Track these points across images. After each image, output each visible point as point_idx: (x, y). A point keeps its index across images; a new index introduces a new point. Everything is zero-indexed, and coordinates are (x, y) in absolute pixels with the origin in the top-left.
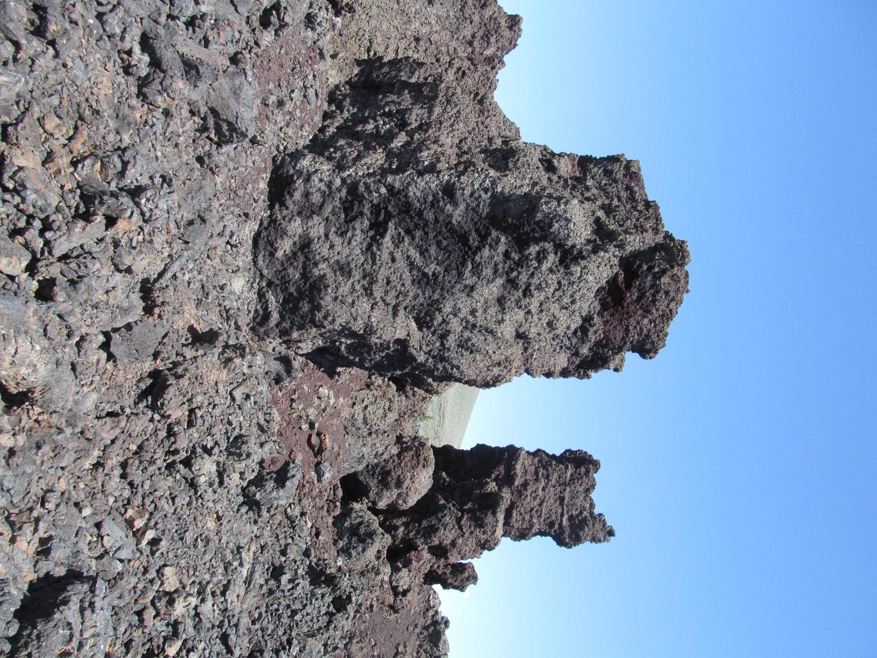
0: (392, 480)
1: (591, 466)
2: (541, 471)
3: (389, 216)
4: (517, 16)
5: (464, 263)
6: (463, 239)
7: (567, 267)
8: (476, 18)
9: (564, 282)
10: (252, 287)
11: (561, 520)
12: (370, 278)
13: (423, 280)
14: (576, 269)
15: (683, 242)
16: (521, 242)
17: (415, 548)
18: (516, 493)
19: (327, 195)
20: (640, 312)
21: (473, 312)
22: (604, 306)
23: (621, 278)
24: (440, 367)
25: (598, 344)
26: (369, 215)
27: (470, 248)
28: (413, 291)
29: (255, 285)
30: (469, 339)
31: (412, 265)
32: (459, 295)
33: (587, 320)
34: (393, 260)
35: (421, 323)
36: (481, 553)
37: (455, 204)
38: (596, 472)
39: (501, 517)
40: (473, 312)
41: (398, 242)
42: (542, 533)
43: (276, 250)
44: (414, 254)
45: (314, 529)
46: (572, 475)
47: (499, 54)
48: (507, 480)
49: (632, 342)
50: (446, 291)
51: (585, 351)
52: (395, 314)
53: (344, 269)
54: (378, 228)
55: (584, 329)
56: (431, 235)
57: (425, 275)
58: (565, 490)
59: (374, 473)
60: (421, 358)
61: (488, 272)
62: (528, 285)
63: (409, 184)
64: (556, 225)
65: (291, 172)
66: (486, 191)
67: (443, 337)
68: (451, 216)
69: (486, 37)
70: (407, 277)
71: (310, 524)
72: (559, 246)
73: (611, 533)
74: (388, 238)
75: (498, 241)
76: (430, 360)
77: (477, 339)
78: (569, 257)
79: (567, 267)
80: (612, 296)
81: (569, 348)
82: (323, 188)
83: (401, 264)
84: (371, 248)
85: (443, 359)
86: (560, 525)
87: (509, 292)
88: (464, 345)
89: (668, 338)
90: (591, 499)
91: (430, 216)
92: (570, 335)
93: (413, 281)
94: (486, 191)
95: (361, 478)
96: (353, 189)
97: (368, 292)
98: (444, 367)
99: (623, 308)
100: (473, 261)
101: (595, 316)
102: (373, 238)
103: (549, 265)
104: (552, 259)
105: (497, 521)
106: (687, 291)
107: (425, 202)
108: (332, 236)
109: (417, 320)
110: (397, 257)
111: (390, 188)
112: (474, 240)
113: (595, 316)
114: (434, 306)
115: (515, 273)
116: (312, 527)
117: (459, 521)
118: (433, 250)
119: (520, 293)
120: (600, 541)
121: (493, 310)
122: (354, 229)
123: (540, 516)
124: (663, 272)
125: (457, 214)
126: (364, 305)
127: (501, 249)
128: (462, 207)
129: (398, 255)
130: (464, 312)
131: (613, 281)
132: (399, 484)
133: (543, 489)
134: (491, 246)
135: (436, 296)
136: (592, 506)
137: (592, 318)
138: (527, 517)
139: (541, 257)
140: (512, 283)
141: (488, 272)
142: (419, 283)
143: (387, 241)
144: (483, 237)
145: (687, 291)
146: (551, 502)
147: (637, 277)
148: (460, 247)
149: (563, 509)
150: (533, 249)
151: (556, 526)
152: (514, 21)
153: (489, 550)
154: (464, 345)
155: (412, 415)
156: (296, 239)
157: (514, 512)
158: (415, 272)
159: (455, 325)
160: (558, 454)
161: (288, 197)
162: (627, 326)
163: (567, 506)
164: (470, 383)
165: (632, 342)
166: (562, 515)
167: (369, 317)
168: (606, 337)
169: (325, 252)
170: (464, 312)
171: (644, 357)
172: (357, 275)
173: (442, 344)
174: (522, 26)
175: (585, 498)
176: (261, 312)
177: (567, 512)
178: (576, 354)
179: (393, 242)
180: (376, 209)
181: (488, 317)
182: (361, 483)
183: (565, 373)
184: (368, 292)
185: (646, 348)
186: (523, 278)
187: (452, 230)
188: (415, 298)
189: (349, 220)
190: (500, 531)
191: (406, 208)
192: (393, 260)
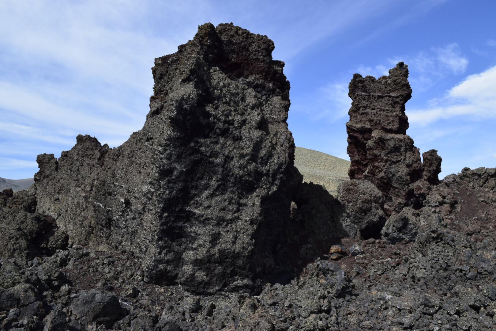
1: (357, 79)
2: (361, 111)
3: (182, 210)
4: (77, 138)
5: (213, 163)
9: (224, 101)
10: (228, 296)
11: (393, 97)
13: (221, 189)
15: (199, 27)
18: (376, 127)
20: (244, 53)
21: (242, 156)
26: (181, 223)
27: (202, 159)
29: (227, 294)
31: (212, 196)
32: (231, 166)
34: (209, 207)
36: (416, 148)
37: (175, 168)
38: (361, 76)
39: (390, 136)
41: (198, 205)
42: (403, 109)
43: (203, 281)
44: (206, 193)
45: (392, 256)
46: (364, 92)
47: (99, 148)
48: (366, 132)
49: (264, 56)
52: (245, 205)
53: (215, 238)
54: (189, 217)
55: (256, 87)
56: (194, 184)
57: (218, 187)
58: (373, 95)
59: (360, 218)
60: (275, 188)
62: (225, 122)
63: (161, 198)
64: (185, 106)
65: (154, 272)
66: (165, 150)
68: (182, 172)
71: (389, 259)
74: (196, 211)
76: (276, 182)
77: (263, 152)
79: (214, 99)
80: (235, 70)
81: (269, 97)
82: (165, 251)
86: (396, 97)
87: (230, 134)
89: (261, 34)
90: (380, 79)
92: (260, 95)
93: (222, 194)
94: (165, 150)
95: (364, 226)
98: (281, 173)
99: (241, 63)
100: (210, 157)
101: (248, 80)
102: (197, 219)
103: (212, 110)
105: (393, 138)
106: (232, 24)
107: (172, 188)
108: (194, 246)
110: (206, 204)
113: (248, 80)
114: (239, 181)
115: (218, 130)
116: (391, 258)
118: (203, 183)
120: (407, 71)
121: (242, 144)
122: (191, 232)
125: (179, 168)
128: (176, 165)
129: (206, 204)
133: (373, 109)
134: (201, 146)
135: (232, 180)
136: (384, 77)
137: (249, 82)
140: (225, 133)
142: (224, 190)
145: (232, 24)
149: (386, 96)
150: (203, 121)
151: (397, 100)
152: (80, 139)
153: (413, 142)
156: (196, 268)
157: (388, 128)
158: (217, 193)
159: (251, 167)
160: (352, 101)
161: (170, 274)
162: (254, 59)
163: (384, 93)
164: (291, 156)
165: (264, 56)
166: (390, 96)
167: (246, 221)
168: (261, 73)
169: (204, 250)
171: (273, 48)
174: (84, 135)
175: (378, 83)
176: (244, 290)
177: (388, 93)
179: (199, 207)
182: (367, 227)
183: (286, 98)
185: (269, 46)
186: (221, 125)
188: (232, 192)
190: (400, 136)
192: (209, 207)
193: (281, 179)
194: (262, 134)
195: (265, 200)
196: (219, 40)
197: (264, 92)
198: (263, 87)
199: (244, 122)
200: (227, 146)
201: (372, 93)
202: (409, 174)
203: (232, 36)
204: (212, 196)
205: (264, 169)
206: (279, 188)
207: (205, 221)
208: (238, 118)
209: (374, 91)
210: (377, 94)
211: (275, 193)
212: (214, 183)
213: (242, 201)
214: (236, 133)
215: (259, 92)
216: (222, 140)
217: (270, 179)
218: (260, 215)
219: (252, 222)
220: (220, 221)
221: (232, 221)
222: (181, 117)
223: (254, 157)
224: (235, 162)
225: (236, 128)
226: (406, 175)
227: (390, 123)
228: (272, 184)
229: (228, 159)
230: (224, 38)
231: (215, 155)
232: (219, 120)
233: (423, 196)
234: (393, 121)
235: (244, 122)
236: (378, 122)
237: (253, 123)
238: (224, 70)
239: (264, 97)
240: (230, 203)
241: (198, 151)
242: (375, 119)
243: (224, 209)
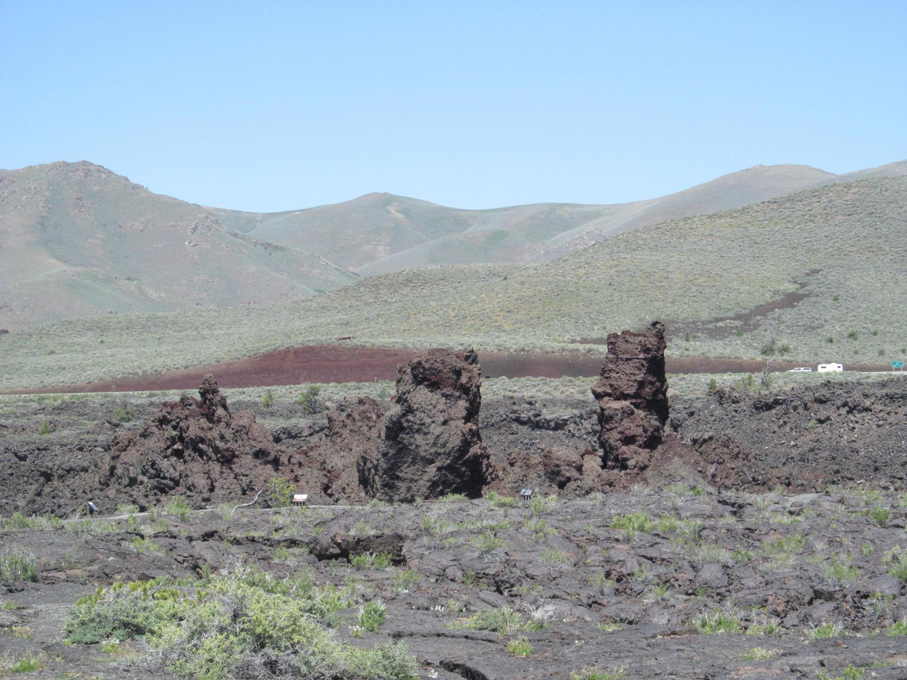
0: (557, 469)
6: (401, 449)
8: (359, 424)
12: (412, 480)
13: (414, 463)
14: (415, 406)
16: (402, 429)
17: (618, 455)
19: (387, 494)
21: (428, 444)
22: (439, 388)
25: (455, 389)
28: (417, 466)
31: (409, 466)
33: (443, 395)
35: (432, 462)
40: (428, 444)
41: (401, 471)
44: (406, 465)
50: (417, 454)
51: (457, 394)
53: (409, 489)
54: (398, 478)
55: (446, 396)
60: (449, 461)
61: (412, 440)
67: (439, 454)
69: (369, 419)
70: (412, 468)
72: (404, 415)
73: (654, 324)
77: (441, 441)
78: (410, 410)
80: (434, 386)
83: (408, 470)
84: (404, 480)
85: (449, 453)
86: (644, 359)
88: (444, 446)
91: (393, 461)
96: (384, 486)
97: (416, 481)
104: (410, 417)
109: (430, 464)
110: (406, 471)
111: (383, 474)
112: (401, 446)
117: (608, 430)
119: (423, 427)
121: (429, 436)
123: (634, 375)
124: (423, 367)
125: (392, 452)
126: (421, 482)
127: (404, 436)
130: (427, 448)
131: (428, 386)
132: (557, 466)
138: (631, 383)
140: (418, 431)
141: (412, 440)
143: (401, 475)
144: (400, 443)
146: (628, 368)
148: (403, 450)
150: (405, 424)
151: (644, 362)
154: (444, 446)
155: (528, 459)
159: (433, 450)
170: (427, 448)
172: (410, 485)
178: (460, 397)
180: (392, 478)
181: (431, 439)
184: (416, 481)
186: (416, 427)
187: (398, 453)
189: (395, 487)
191: (390, 469)
195: (439, 469)
198: (452, 395)
200: (419, 438)
206: (452, 461)
207: (404, 480)
211: (449, 465)
212: (410, 460)
214: (426, 430)
216: (416, 436)
219: (428, 481)
220: (412, 480)
223: (435, 444)
224: (422, 448)
231: (411, 444)
233: (627, 459)
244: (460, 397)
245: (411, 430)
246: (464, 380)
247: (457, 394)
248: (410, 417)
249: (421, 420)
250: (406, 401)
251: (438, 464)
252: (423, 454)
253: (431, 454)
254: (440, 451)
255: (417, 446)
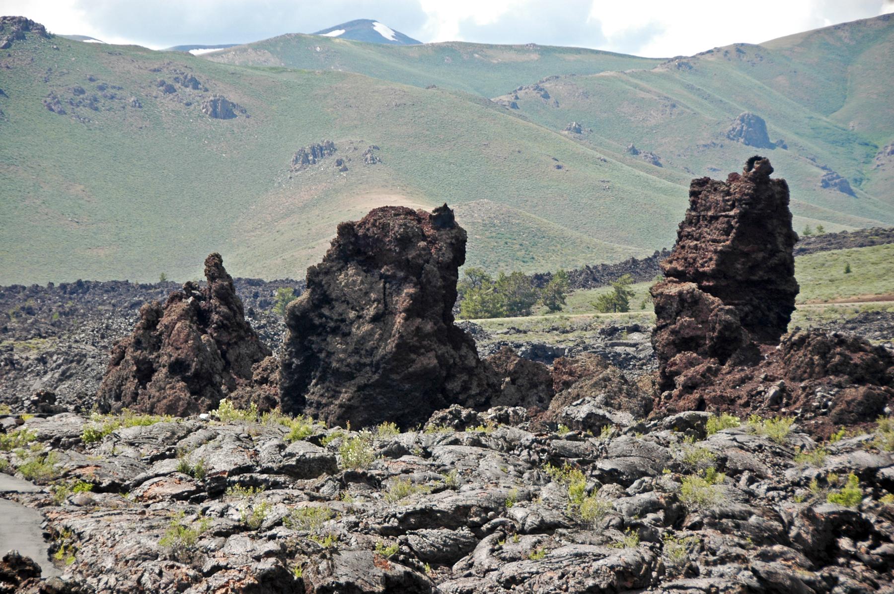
7: (332, 300)
14: (334, 296)
23: (361, 258)
24: (382, 366)
28: (327, 384)
30: (367, 351)
31: (316, 385)
35: (350, 377)
44: (314, 381)
51: (401, 274)
55: (385, 278)
57: (320, 377)
58: (704, 216)
60: (376, 377)
61: (323, 345)
62: (337, 321)
67: (365, 365)
68: (297, 365)
75: (310, 340)
85: (378, 364)
88: (371, 353)
100: (318, 352)
119: (343, 326)
121: (349, 339)
127: (314, 338)
139: (321, 316)
140: (335, 331)
147: (359, 250)
150: (317, 321)
159: (352, 360)
173: (369, 365)
186: (332, 324)
188: (330, 382)
192: (313, 393)
193: (384, 368)
194: (372, 329)
196: (356, 235)
197: (394, 282)
198: (394, 276)
199: (359, 317)
201: (703, 213)
202: (668, 344)
203: (368, 230)
204: (316, 385)
205: (368, 361)
208: (352, 314)
209: (709, 209)
210: (710, 213)
211: (377, 381)
212: (318, 374)
213: (338, 389)
215: (390, 283)
217: (374, 370)
218: (349, 400)
221: (326, 405)
222: (292, 322)
223: (356, 351)
225: (347, 325)
226: (663, 346)
227: (706, 262)
228: (374, 373)
229: (329, 354)
230: (361, 232)
231: (320, 351)
232: (332, 319)
234: (711, 259)
235: (359, 317)
236: (692, 261)
237: (367, 318)
238: (360, 263)
239: (394, 287)
240: (327, 391)
241: (311, 348)
242: (690, 255)
243: (322, 395)
244: (405, 280)
245: (322, 331)
246: (411, 254)
247: (401, 274)
248: (326, 311)
249: (341, 315)
250: (320, 285)
251: (361, 380)
252: (334, 364)
253: (348, 365)
254: (364, 360)
255: (329, 354)
